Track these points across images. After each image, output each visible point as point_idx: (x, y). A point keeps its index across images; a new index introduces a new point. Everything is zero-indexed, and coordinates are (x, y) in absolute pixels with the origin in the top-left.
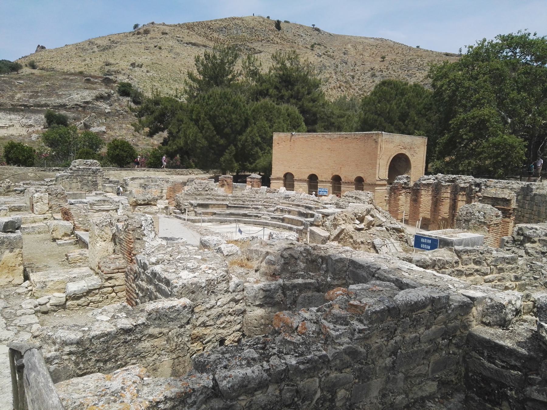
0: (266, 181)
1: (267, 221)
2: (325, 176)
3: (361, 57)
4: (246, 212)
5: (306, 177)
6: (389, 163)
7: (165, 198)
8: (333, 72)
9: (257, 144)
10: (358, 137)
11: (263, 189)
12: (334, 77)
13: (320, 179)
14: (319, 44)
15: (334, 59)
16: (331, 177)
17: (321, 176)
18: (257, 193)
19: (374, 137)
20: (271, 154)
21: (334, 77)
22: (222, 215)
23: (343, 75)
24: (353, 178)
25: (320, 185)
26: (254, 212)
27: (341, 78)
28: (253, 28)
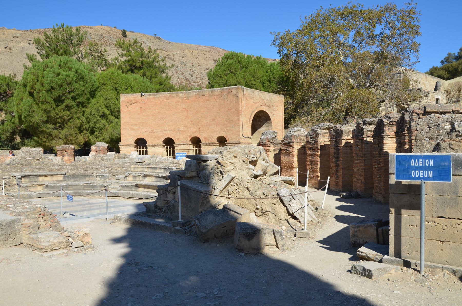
1: (117, 191)
3: (197, 59)
5: (161, 141)
8: (174, 72)
9: (103, 116)
10: (216, 94)
11: (110, 155)
12: (176, 75)
14: (160, 49)
15: (175, 61)
17: (178, 139)
18: (102, 160)
19: (234, 92)
21: (176, 75)
22: (57, 187)
23: (183, 74)
26: (99, 181)
27: (181, 76)
28: (102, 35)
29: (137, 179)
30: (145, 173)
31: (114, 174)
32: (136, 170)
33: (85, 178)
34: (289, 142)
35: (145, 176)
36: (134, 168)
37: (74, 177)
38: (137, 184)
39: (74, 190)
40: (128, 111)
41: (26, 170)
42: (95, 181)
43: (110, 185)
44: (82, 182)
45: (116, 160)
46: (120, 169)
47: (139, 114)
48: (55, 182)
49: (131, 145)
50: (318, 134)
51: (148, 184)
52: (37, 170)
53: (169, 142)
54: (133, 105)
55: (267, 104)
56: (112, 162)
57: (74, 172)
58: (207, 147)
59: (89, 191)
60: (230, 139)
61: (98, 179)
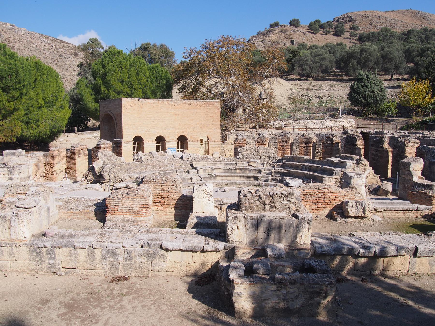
7: (31, 177)
10: (201, 104)
13: (166, 139)
17: (168, 137)
34: (263, 142)
36: (196, 164)
49: (131, 142)
50: (289, 138)
53: (160, 140)
58: (192, 143)
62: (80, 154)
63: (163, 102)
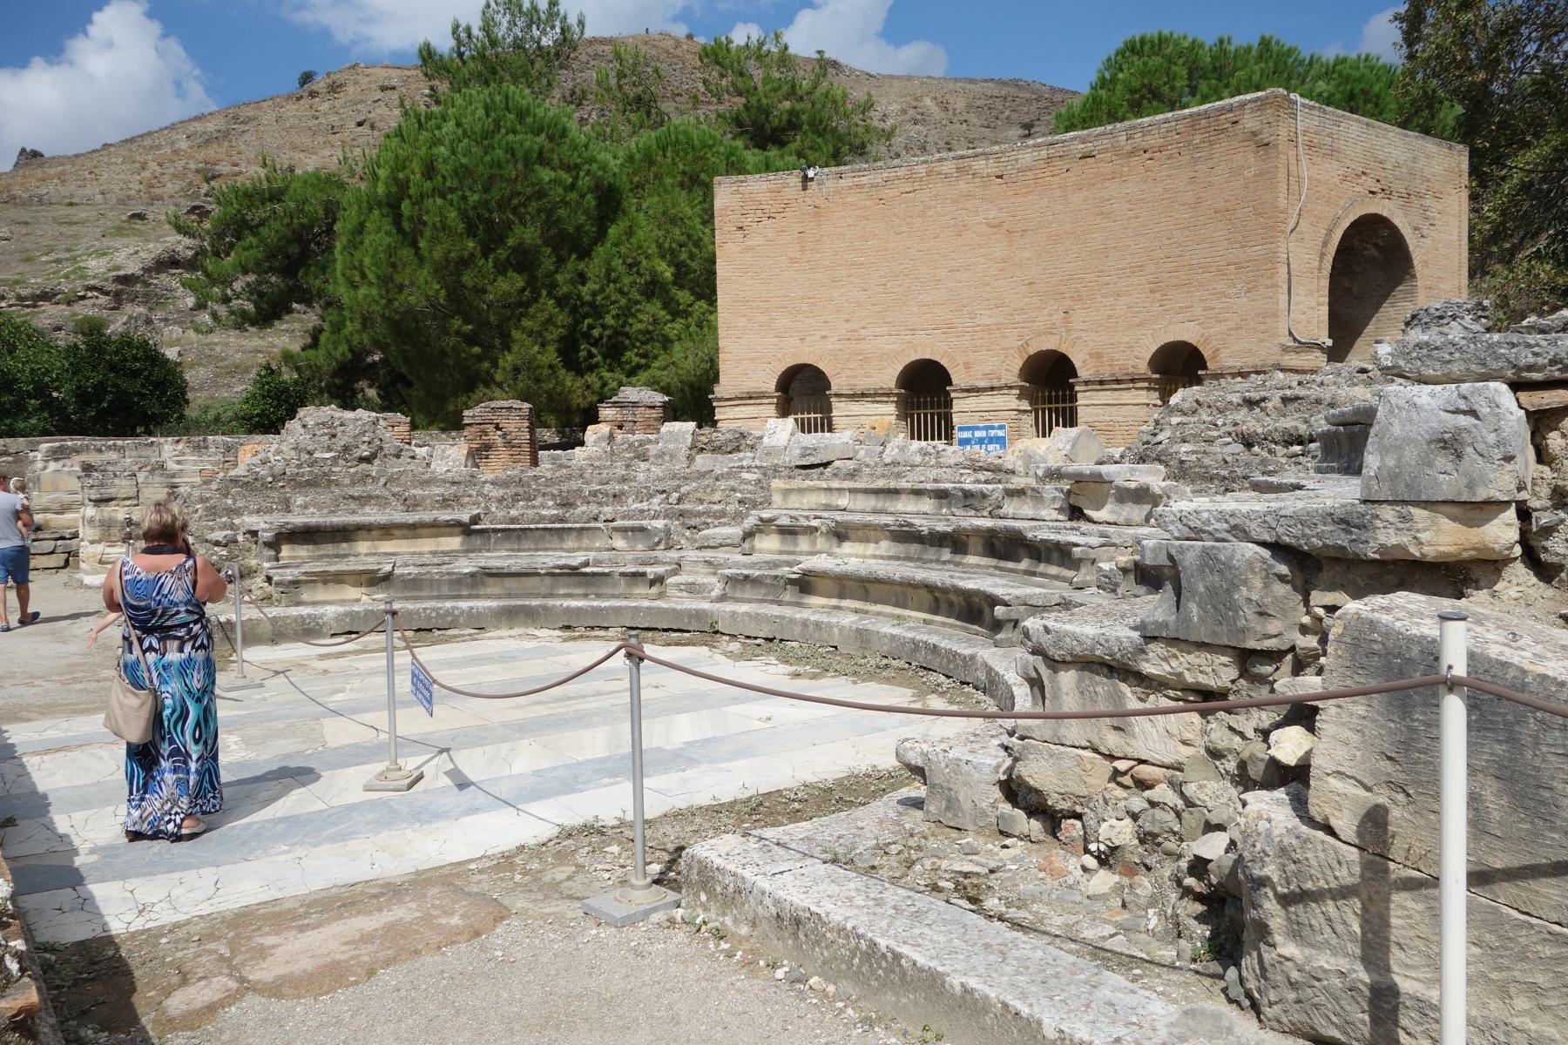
0: (694, 401)
1: (706, 605)
2: (985, 363)
4: (576, 559)
5: (888, 377)
6: (1330, 258)
10: (1153, 141)
13: (959, 378)
16: (1018, 363)
17: (967, 365)
19: (1250, 122)
20: (713, 329)
22: (433, 583)
24: (1139, 355)
25: (963, 410)
26: (625, 554)
29: (803, 543)
30: (838, 516)
31: (692, 522)
32: (794, 501)
33: (561, 540)
35: (840, 534)
36: (786, 493)
37: (514, 535)
38: (807, 574)
39: (509, 596)
40: (748, 249)
41: (305, 507)
42: (606, 555)
43: (675, 573)
44: (549, 558)
45: (702, 462)
46: (717, 496)
47: (793, 261)
48: (426, 559)
51: (863, 573)
52: (353, 506)
54: (766, 222)
55: (1398, 186)
56: (680, 466)
57: (513, 512)
59: (574, 603)
60: (1224, 354)
61: (619, 543)
62: (487, 447)
63: (938, 167)
